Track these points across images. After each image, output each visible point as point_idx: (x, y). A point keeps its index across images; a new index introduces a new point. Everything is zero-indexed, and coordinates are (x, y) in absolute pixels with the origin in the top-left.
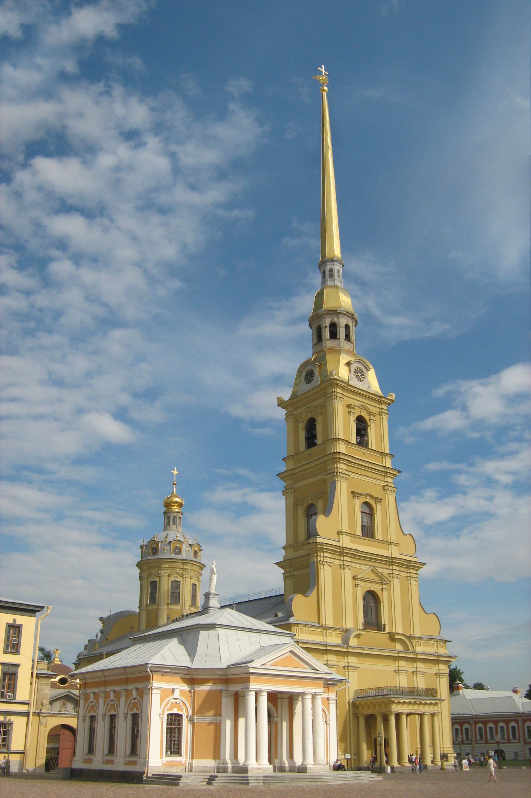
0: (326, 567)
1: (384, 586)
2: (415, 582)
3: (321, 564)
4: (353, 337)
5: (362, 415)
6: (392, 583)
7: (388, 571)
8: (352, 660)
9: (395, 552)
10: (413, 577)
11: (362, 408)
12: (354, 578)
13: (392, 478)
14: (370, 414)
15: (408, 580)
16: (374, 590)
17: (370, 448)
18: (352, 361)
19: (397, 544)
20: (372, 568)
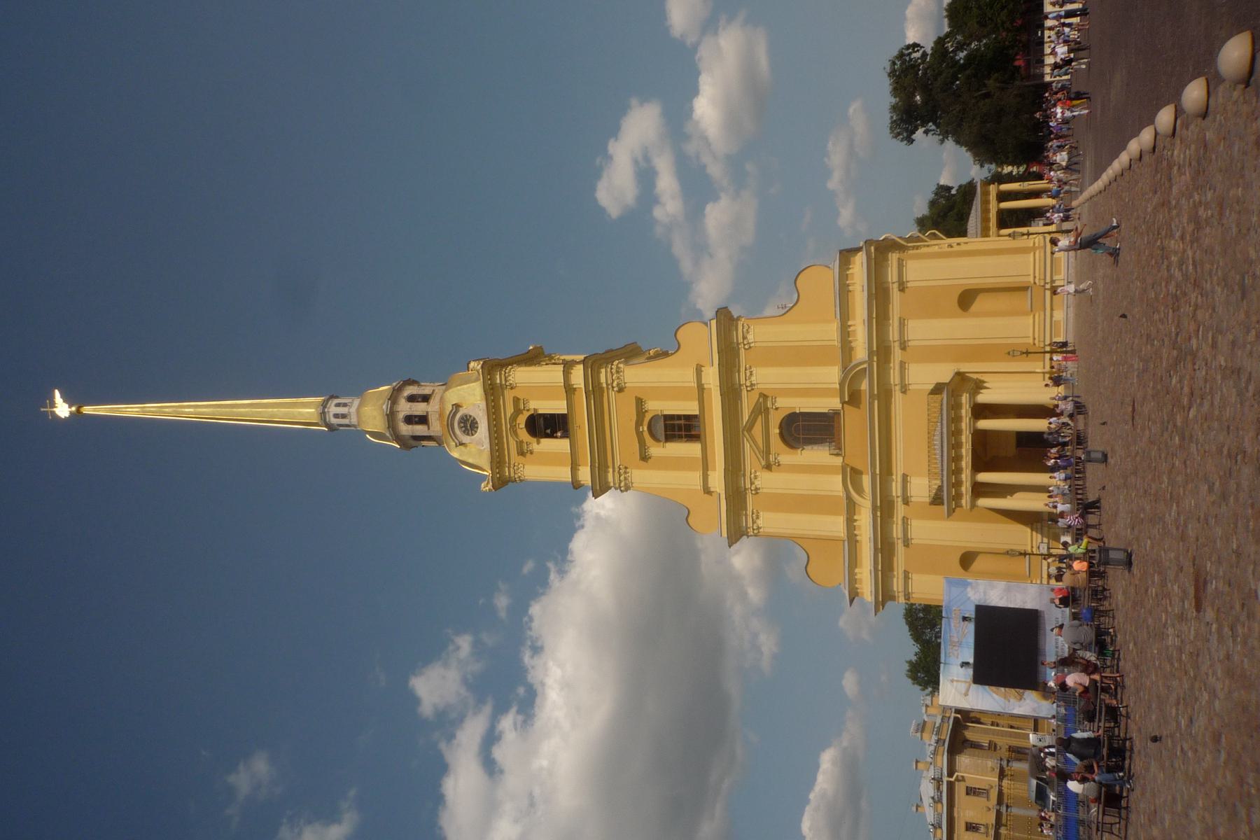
0: (760, 522)
1: (769, 405)
2: (751, 332)
3: (759, 532)
4: (419, 409)
5: (523, 425)
6: (759, 386)
7: (744, 393)
8: (896, 489)
9: (712, 377)
10: (744, 338)
11: (515, 426)
12: (768, 467)
13: (599, 373)
14: (518, 411)
15: (750, 347)
16: (778, 427)
17: (566, 412)
18: (456, 444)
19: (699, 370)
20: (746, 433)
